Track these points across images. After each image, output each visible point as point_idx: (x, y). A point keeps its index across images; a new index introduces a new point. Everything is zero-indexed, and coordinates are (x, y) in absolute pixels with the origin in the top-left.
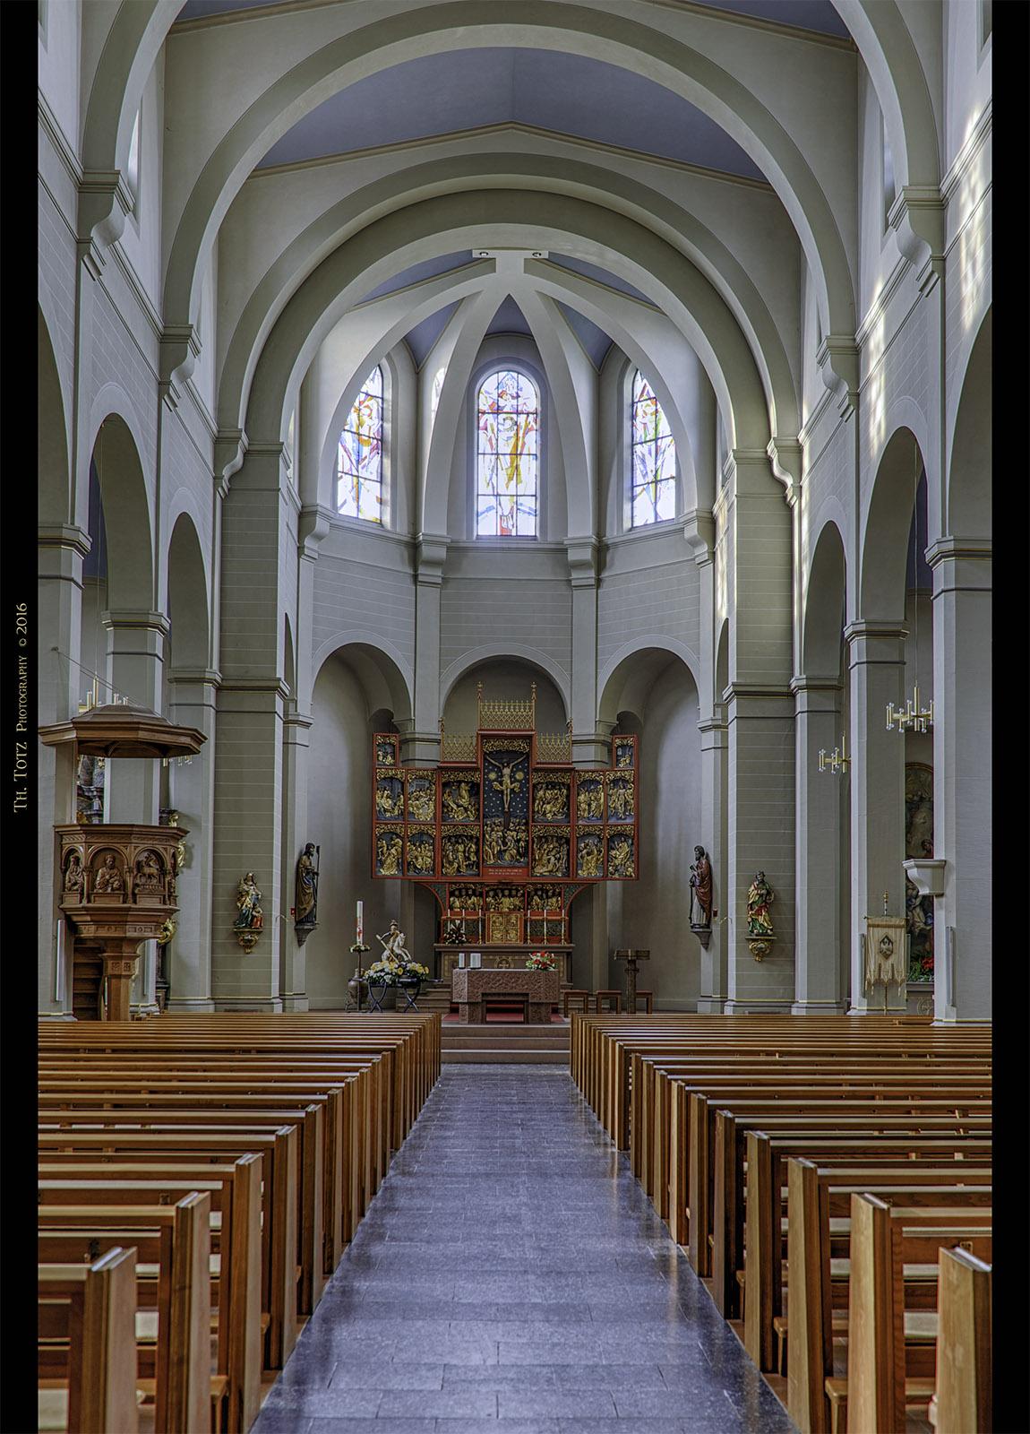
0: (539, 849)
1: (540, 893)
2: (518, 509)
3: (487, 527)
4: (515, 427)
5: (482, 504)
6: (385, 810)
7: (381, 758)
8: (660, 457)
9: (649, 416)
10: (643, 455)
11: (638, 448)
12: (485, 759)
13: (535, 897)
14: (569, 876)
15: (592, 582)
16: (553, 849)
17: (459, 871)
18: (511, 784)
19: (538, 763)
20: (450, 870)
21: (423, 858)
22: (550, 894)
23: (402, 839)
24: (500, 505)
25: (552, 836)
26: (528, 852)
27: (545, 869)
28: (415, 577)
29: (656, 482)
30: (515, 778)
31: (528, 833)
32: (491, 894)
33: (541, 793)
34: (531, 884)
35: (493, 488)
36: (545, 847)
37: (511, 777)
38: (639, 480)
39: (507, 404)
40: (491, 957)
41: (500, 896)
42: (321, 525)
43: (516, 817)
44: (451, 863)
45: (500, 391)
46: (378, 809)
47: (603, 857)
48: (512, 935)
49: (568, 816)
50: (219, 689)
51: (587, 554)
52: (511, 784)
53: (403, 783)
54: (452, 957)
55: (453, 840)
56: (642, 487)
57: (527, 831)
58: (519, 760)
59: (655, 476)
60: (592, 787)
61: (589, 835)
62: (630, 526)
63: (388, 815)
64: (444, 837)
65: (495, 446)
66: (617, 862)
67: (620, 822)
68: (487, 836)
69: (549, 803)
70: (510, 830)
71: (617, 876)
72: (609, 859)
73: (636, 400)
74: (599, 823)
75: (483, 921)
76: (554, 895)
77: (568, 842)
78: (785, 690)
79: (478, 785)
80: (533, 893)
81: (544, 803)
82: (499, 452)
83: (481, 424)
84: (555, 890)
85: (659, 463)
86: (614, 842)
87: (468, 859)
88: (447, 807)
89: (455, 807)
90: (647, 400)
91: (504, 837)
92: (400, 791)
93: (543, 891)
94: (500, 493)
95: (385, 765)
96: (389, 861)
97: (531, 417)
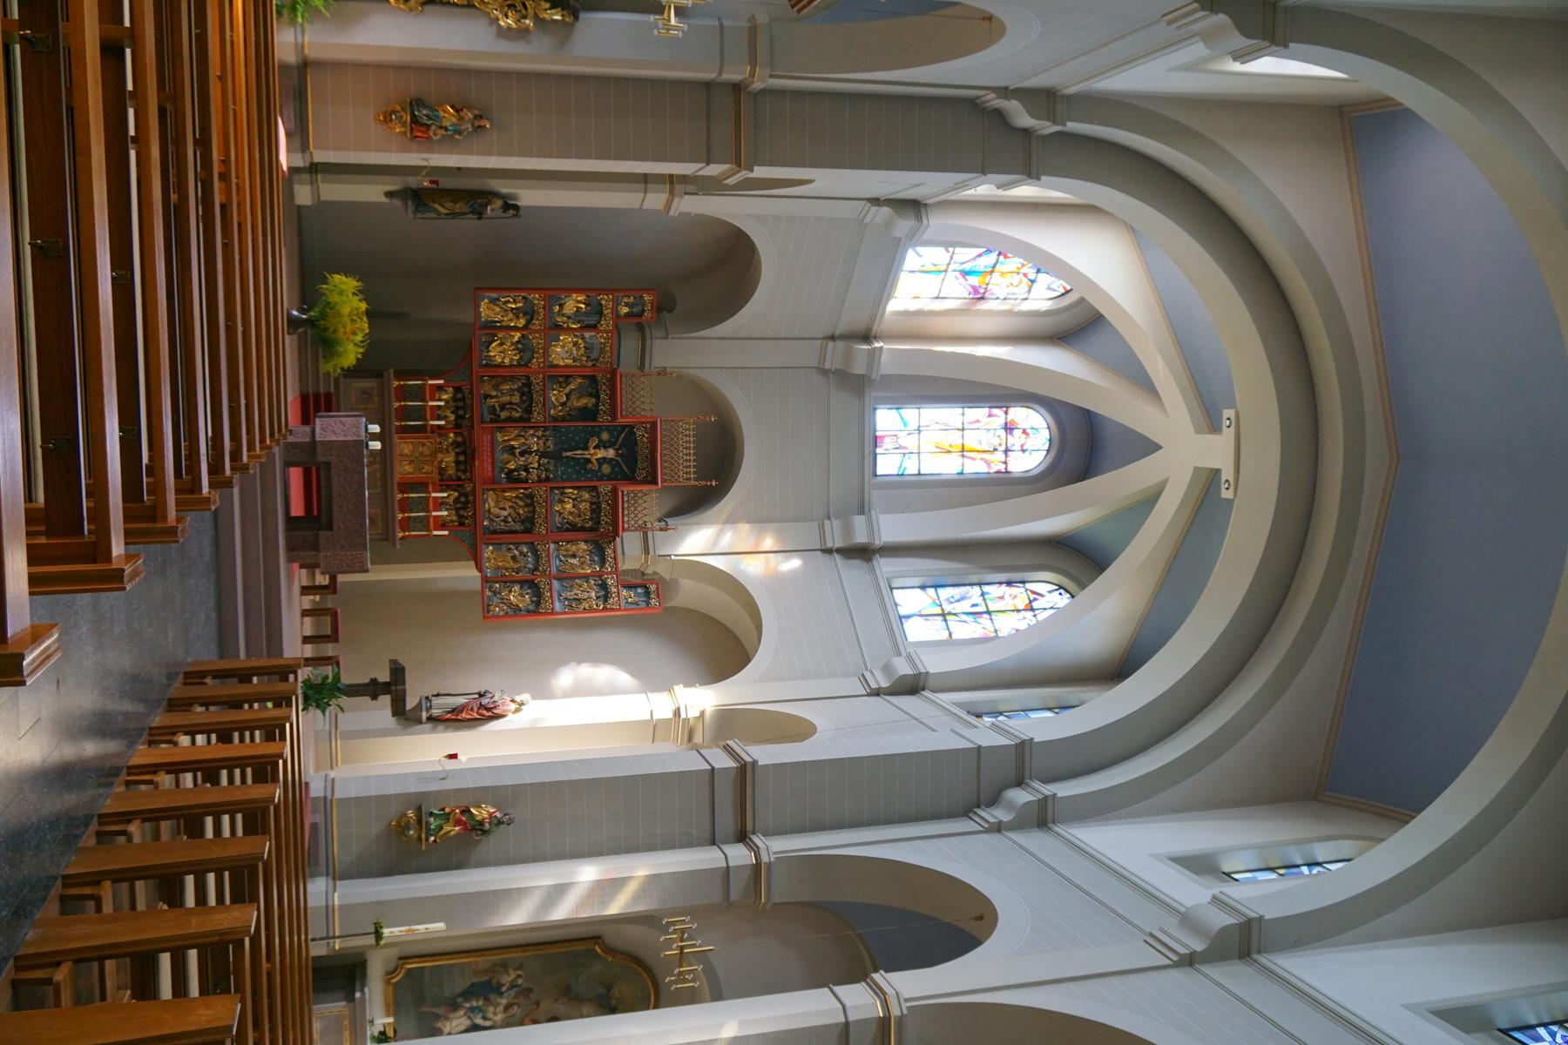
0: (517, 497)
1: (463, 499)
2: (904, 454)
3: (886, 419)
5: (910, 413)
6: (561, 306)
7: (626, 300)
8: (970, 618)
9: (1012, 602)
10: (970, 598)
11: (977, 589)
12: (623, 427)
13: (456, 494)
15: (829, 545)
16: (519, 514)
17: (487, 396)
19: (623, 492)
20: (486, 388)
21: (501, 353)
22: (462, 512)
23: (526, 327)
24: (909, 434)
25: (534, 512)
27: (492, 504)
28: (833, 338)
29: (943, 615)
30: (603, 464)
31: (538, 481)
32: (460, 439)
33: (587, 496)
35: (927, 426)
36: (522, 503)
37: (604, 459)
38: (945, 593)
39: (1016, 439)
41: (457, 450)
42: (904, 225)
43: (555, 466)
44: (496, 387)
45: (1029, 431)
46: (563, 296)
47: (511, 575)
48: (408, 468)
49: (560, 530)
50: (737, 88)
51: (861, 538)
53: (594, 327)
54: (376, 392)
55: (526, 390)
56: (935, 597)
57: (539, 481)
58: (625, 468)
59: (950, 613)
60: (596, 558)
61: (537, 558)
62: (893, 586)
64: (528, 377)
68: (531, 432)
69: (574, 506)
72: (508, 582)
73: (1028, 586)
74: (554, 570)
76: (460, 517)
77: (528, 531)
78: (749, 827)
79: (595, 419)
80: (462, 491)
81: (573, 500)
82: (965, 431)
83: (995, 411)
84: (466, 518)
85: (964, 617)
86: (529, 588)
87: (503, 407)
88: (566, 381)
89: (567, 390)
90: (1029, 598)
92: (586, 322)
93: (466, 506)
94: (922, 433)
96: (498, 309)
97: (1002, 467)
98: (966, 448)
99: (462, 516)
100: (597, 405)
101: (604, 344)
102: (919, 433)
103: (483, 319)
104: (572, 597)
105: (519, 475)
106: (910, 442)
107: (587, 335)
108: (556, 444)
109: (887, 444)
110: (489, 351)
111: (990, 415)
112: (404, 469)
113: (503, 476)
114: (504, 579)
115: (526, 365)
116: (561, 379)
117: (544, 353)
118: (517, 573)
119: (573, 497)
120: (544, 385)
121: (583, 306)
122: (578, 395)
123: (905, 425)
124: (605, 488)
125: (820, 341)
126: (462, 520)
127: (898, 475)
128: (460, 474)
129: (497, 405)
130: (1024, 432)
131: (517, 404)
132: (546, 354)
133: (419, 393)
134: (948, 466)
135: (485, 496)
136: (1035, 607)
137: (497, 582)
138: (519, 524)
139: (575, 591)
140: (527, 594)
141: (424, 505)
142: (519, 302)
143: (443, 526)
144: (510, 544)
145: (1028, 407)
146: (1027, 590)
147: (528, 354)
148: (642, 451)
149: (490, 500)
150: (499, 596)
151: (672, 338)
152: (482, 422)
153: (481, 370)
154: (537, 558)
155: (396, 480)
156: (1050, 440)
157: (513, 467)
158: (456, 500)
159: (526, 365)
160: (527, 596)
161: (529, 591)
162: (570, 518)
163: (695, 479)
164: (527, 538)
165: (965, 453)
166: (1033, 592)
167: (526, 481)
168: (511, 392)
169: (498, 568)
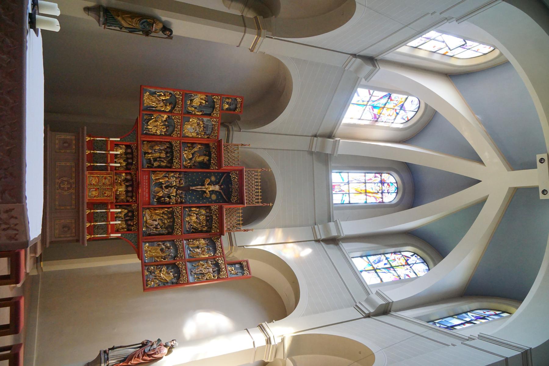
0: (163, 213)
1: (130, 214)
2: (343, 194)
3: (336, 177)
4: (377, 192)
5: (344, 175)
6: (192, 101)
10: (382, 261)
11: (383, 257)
12: (224, 173)
13: (126, 211)
14: (143, 236)
15: (319, 237)
16: (164, 223)
17: (146, 153)
18: (209, 191)
20: (145, 148)
22: (129, 222)
23: (170, 112)
24: (345, 184)
25: (174, 222)
26: (161, 204)
27: (148, 218)
28: (315, 136)
30: (212, 194)
31: (175, 204)
32: (129, 177)
33: (203, 212)
34: (138, 207)
36: (166, 217)
37: (213, 191)
38: (372, 258)
39: (386, 186)
40: (74, 175)
41: (126, 184)
43: (185, 195)
44: (152, 148)
45: (390, 184)
46: (193, 95)
51: (334, 233)
52: (209, 191)
53: (209, 115)
54: (74, 142)
55: (169, 150)
60: (211, 248)
61: (176, 249)
63: (189, 102)
64: (170, 143)
65: (369, 182)
66: (157, 272)
67: (189, 273)
68: (172, 174)
69: (197, 218)
70: (177, 191)
71: (146, 273)
72: (159, 266)
73: (402, 253)
74: (187, 257)
75: (105, 169)
76: (128, 225)
80: (130, 209)
81: (196, 214)
82: (367, 184)
83: (377, 175)
84: (133, 226)
85: (384, 270)
86: (172, 268)
89: (193, 152)
91: (171, 187)
92: (205, 112)
94: (350, 184)
95: (223, 103)
96: (154, 99)
97: (381, 200)
98: (367, 192)
99: (130, 225)
100: (209, 160)
101: (215, 125)
102: (348, 184)
103: (145, 105)
104: (198, 273)
105: (165, 200)
106: (345, 188)
107: (205, 119)
108: (185, 183)
109: (337, 189)
110: (149, 125)
111: (375, 177)
112: (92, 194)
113: (155, 200)
114: (156, 263)
115: (170, 135)
116: (189, 145)
117: (180, 128)
118: (164, 259)
119: (196, 213)
120: (180, 147)
121: (204, 102)
122: (198, 155)
123: (343, 180)
124: (214, 207)
125: (311, 137)
126: (130, 227)
127: (341, 204)
128: (128, 198)
129: (151, 158)
130: (388, 184)
131: (163, 158)
132: (181, 130)
133: (103, 146)
134: (359, 200)
135: (144, 213)
136: (409, 263)
137: (152, 266)
138: (164, 229)
139: (200, 269)
140: (171, 272)
141: (105, 217)
142: (168, 96)
143: (117, 231)
144: (159, 242)
145: (389, 174)
146: (403, 256)
147: (171, 129)
148: (235, 186)
149: (147, 215)
150: (153, 274)
151: (243, 131)
152: (143, 168)
153: (143, 136)
154: (176, 249)
155: (86, 201)
156: (397, 188)
157: (161, 195)
158: (126, 215)
159: (170, 135)
160: (171, 274)
161: (172, 270)
162: (195, 225)
163: (261, 202)
164: (170, 238)
165: (367, 194)
166: (406, 257)
167: (169, 203)
168: (160, 151)
169: (152, 257)
